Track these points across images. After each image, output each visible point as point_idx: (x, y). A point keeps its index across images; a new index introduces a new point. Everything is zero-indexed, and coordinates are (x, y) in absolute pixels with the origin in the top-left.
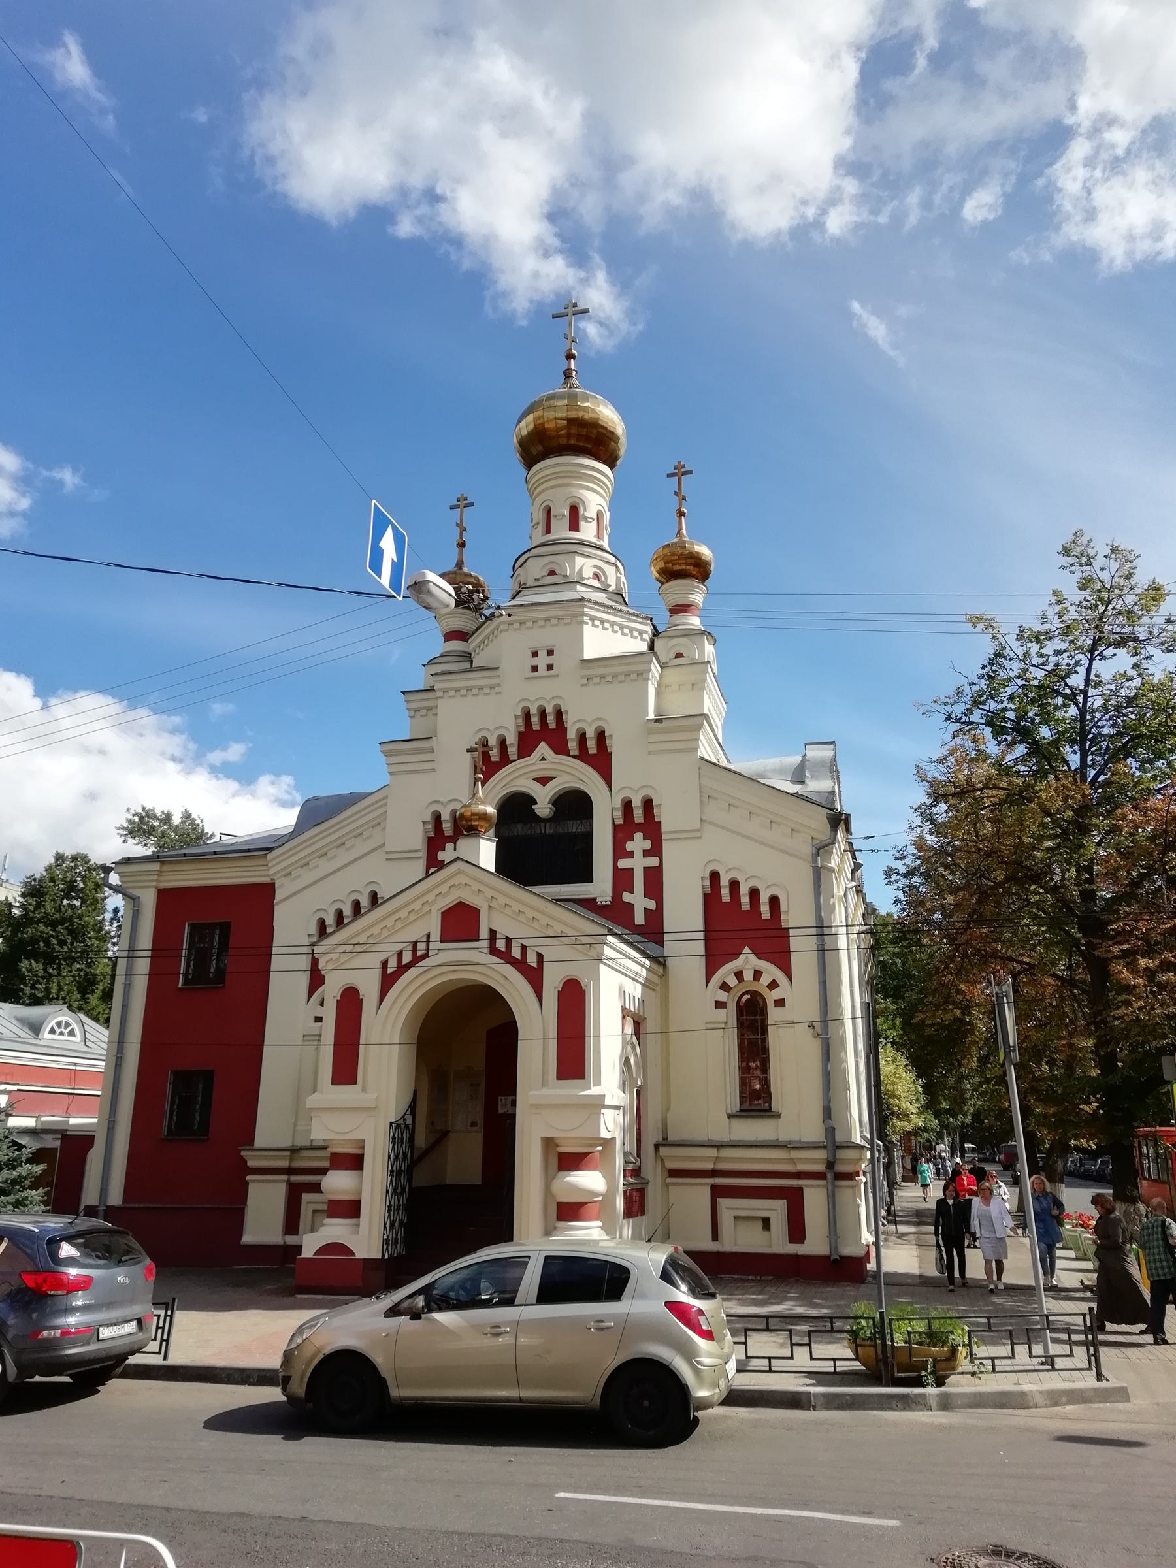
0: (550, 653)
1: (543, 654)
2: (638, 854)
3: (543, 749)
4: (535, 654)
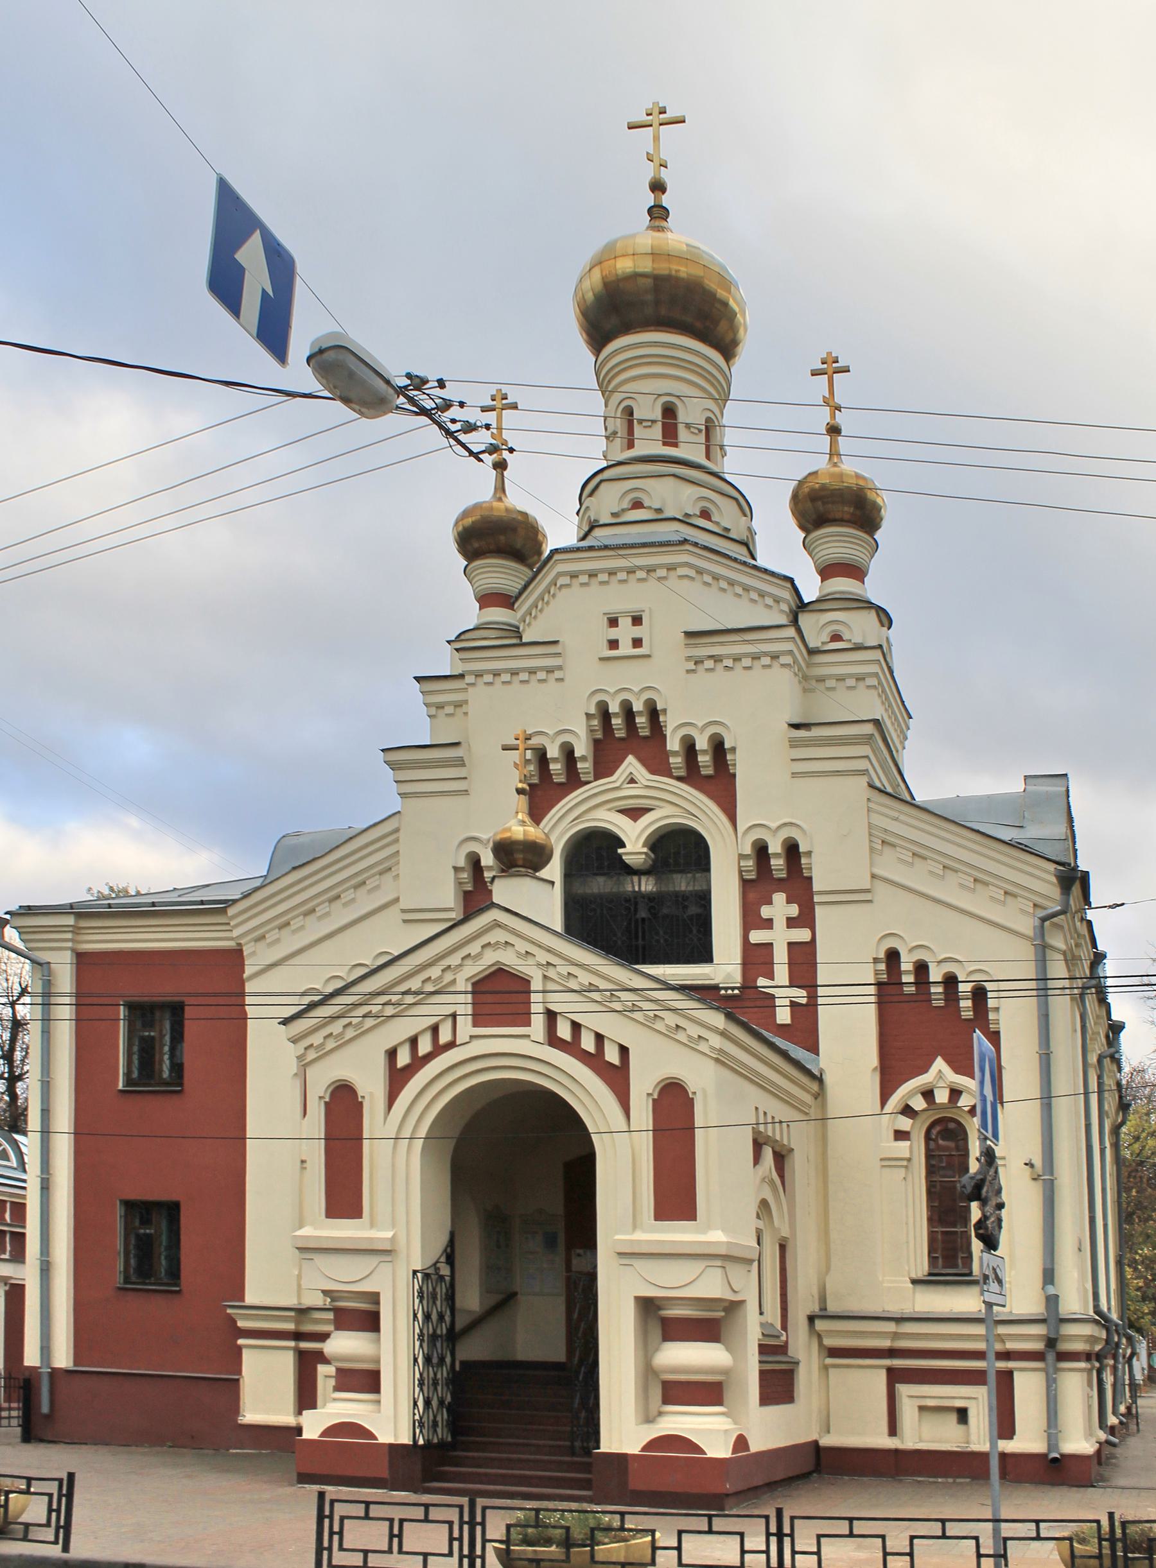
4: (613, 622)
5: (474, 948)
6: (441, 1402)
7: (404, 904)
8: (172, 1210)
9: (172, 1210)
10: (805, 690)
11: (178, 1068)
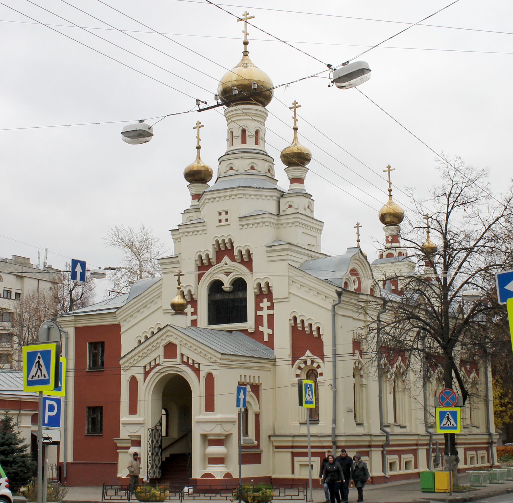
0: (227, 213)
1: (223, 213)
2: (265, 308)
3: (226, 259)
5: (164, 337)
6: (157, 466)
7: (164, 308)
8: (101, 408)
9: (101, 408)
10: (277, 228)
11: (103, 363)
